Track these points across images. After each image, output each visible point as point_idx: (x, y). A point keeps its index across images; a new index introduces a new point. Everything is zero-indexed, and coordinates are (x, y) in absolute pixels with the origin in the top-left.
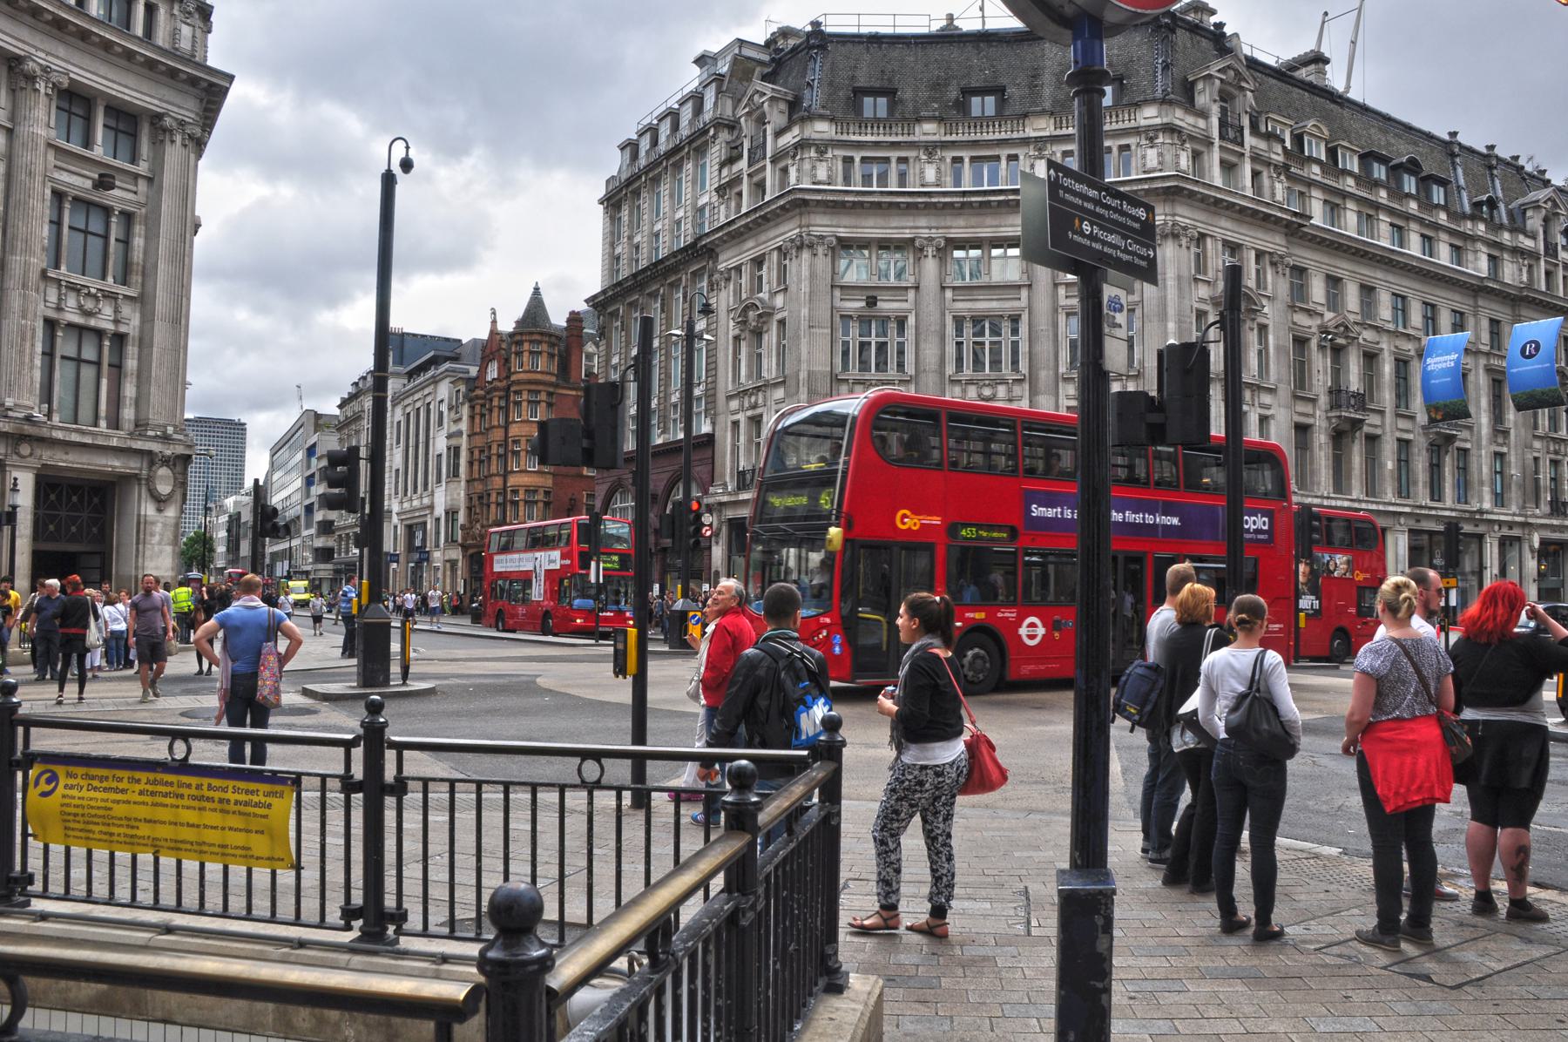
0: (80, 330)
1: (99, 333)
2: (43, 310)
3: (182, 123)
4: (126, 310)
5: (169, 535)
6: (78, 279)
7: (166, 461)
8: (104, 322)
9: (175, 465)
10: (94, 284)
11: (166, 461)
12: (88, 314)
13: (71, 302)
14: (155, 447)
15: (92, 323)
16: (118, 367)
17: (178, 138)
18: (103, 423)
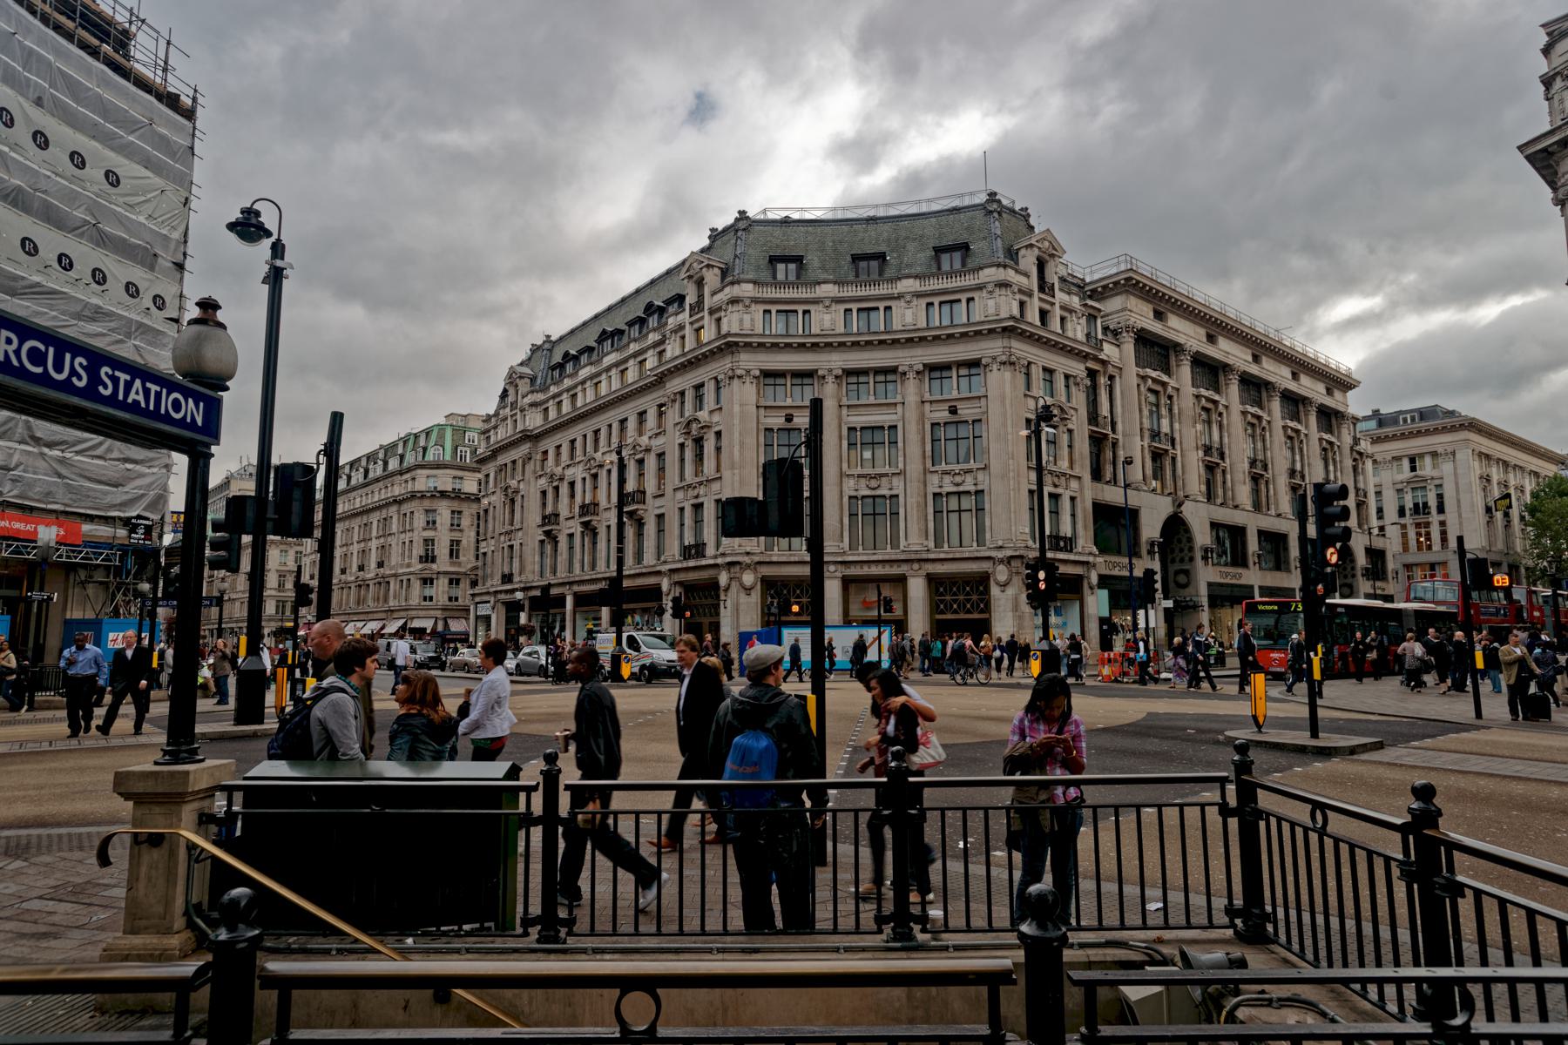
0: (959, 494)
1: (968, 493)
2: (932, 489)
3: (994, 358)
4: (980, 475)
5: (1010, 606)
6: (949, 468)
7: (1001, 561)
8: (969, 486)
9: (1009, 563)
10: (957, 468)
11: (1001, 561)
12: (958, 485)
13: (947, 479)
14: (993, 554)
15: (961, 489)
16: (980, 510)
17: (995, 367)
18: (975, 544)
